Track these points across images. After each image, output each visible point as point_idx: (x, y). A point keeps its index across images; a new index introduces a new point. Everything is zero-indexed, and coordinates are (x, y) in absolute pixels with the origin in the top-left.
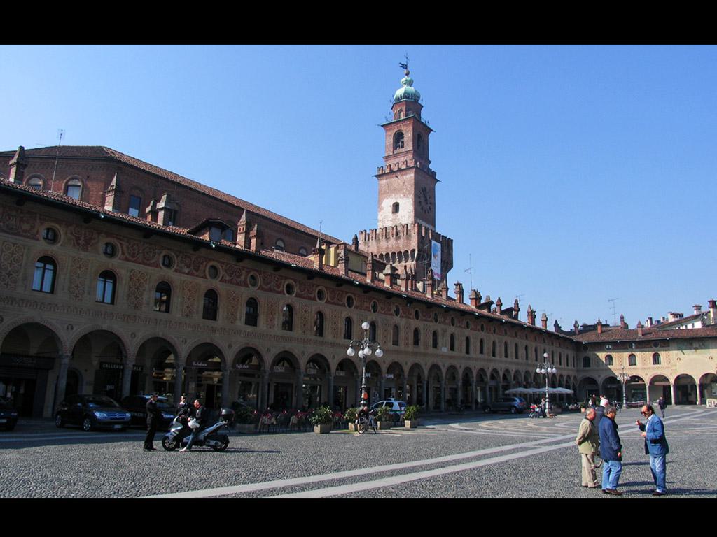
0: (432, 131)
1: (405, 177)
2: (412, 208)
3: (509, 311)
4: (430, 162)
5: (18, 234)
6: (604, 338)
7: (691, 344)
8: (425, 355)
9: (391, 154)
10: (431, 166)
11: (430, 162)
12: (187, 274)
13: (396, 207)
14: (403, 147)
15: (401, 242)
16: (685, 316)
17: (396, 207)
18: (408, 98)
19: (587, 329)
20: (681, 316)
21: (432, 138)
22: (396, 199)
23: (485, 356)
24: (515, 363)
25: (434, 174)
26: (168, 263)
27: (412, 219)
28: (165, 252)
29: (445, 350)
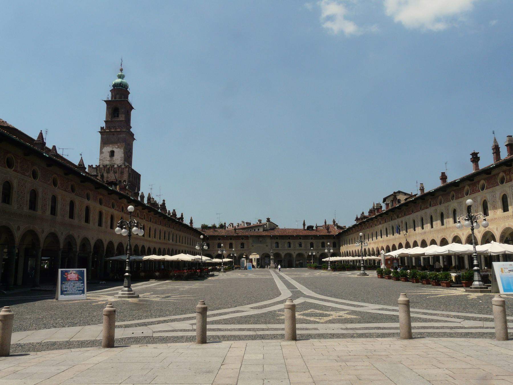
0: (133, 108)
1: (119, 136)
2: (123, 155)
3: (179, 219)
4: (131, 127)
5: (81, 197)
6: (216, 234)
7: (259, 239)
8: (166, 244)
9: (110, 120)
10: (131, 130)
11: (131, 127)
12: (118, 210)
13: (112, 154)
14: (118, 116)
15: (117, 175)
16: (252, 224)
17: (112, 154)
18: (122, 86)
19: (204, 227)
20: (250, 224)
21: (133, 112)
22: (113, 148)
23: (184, 244)
24: (188, 247)
25: (133, 135)
26: (113, 207)
27: (122, 162)
28: (113, 201)
29: (171, 241)
